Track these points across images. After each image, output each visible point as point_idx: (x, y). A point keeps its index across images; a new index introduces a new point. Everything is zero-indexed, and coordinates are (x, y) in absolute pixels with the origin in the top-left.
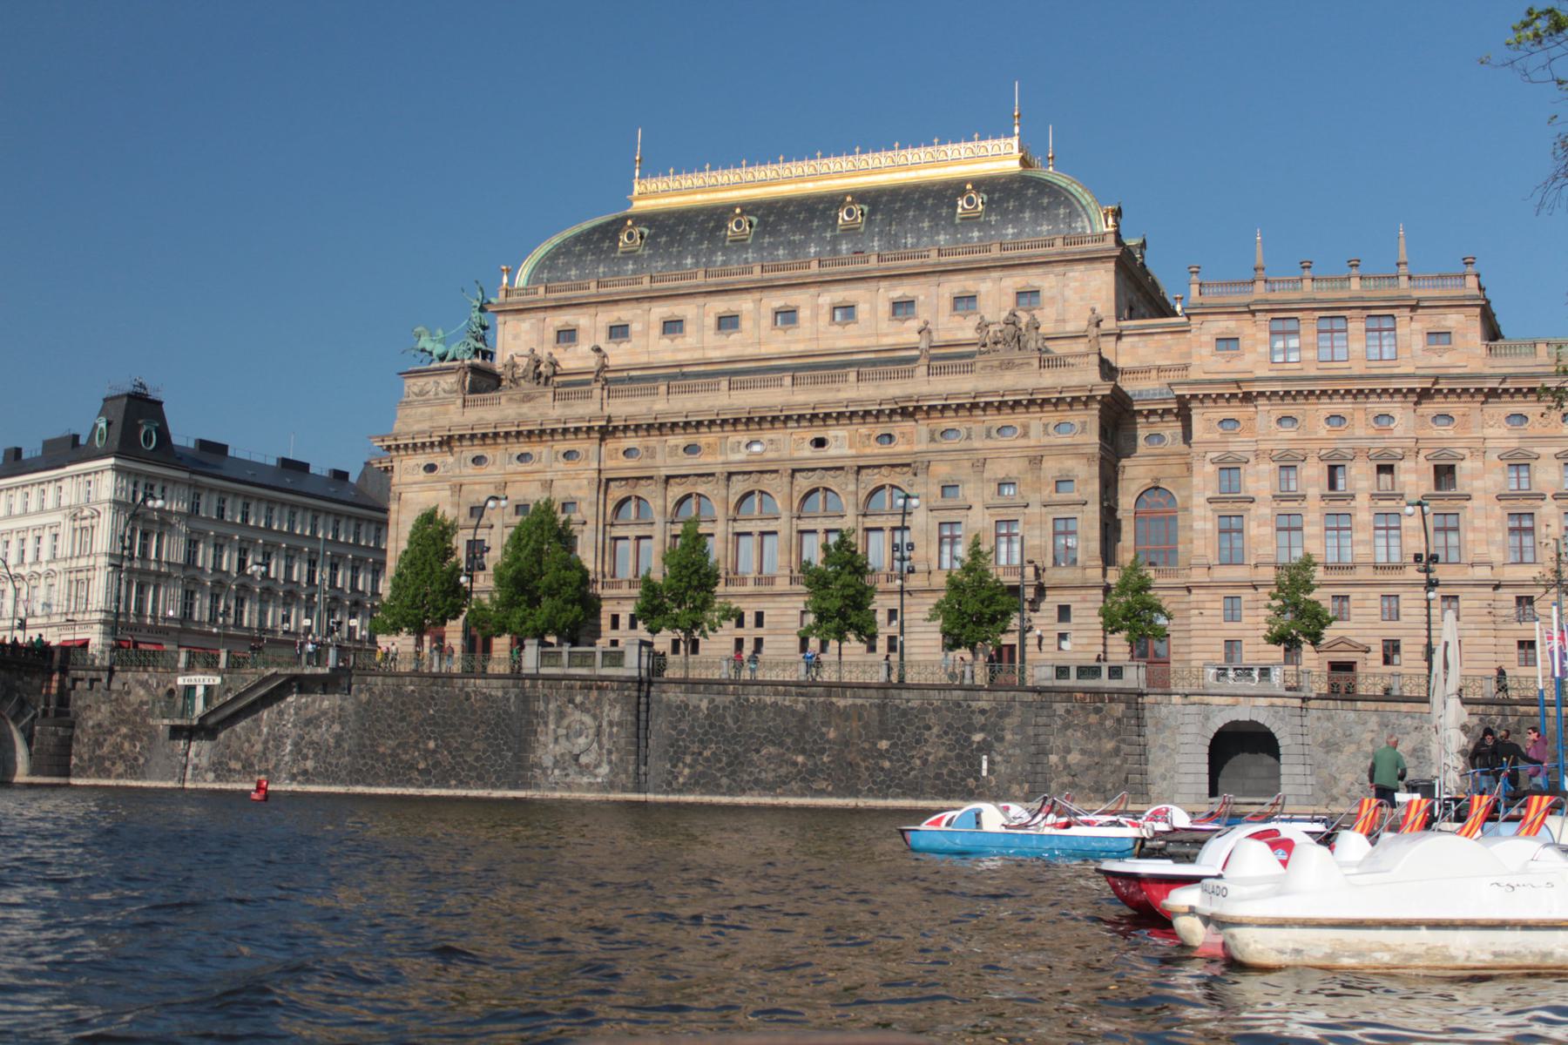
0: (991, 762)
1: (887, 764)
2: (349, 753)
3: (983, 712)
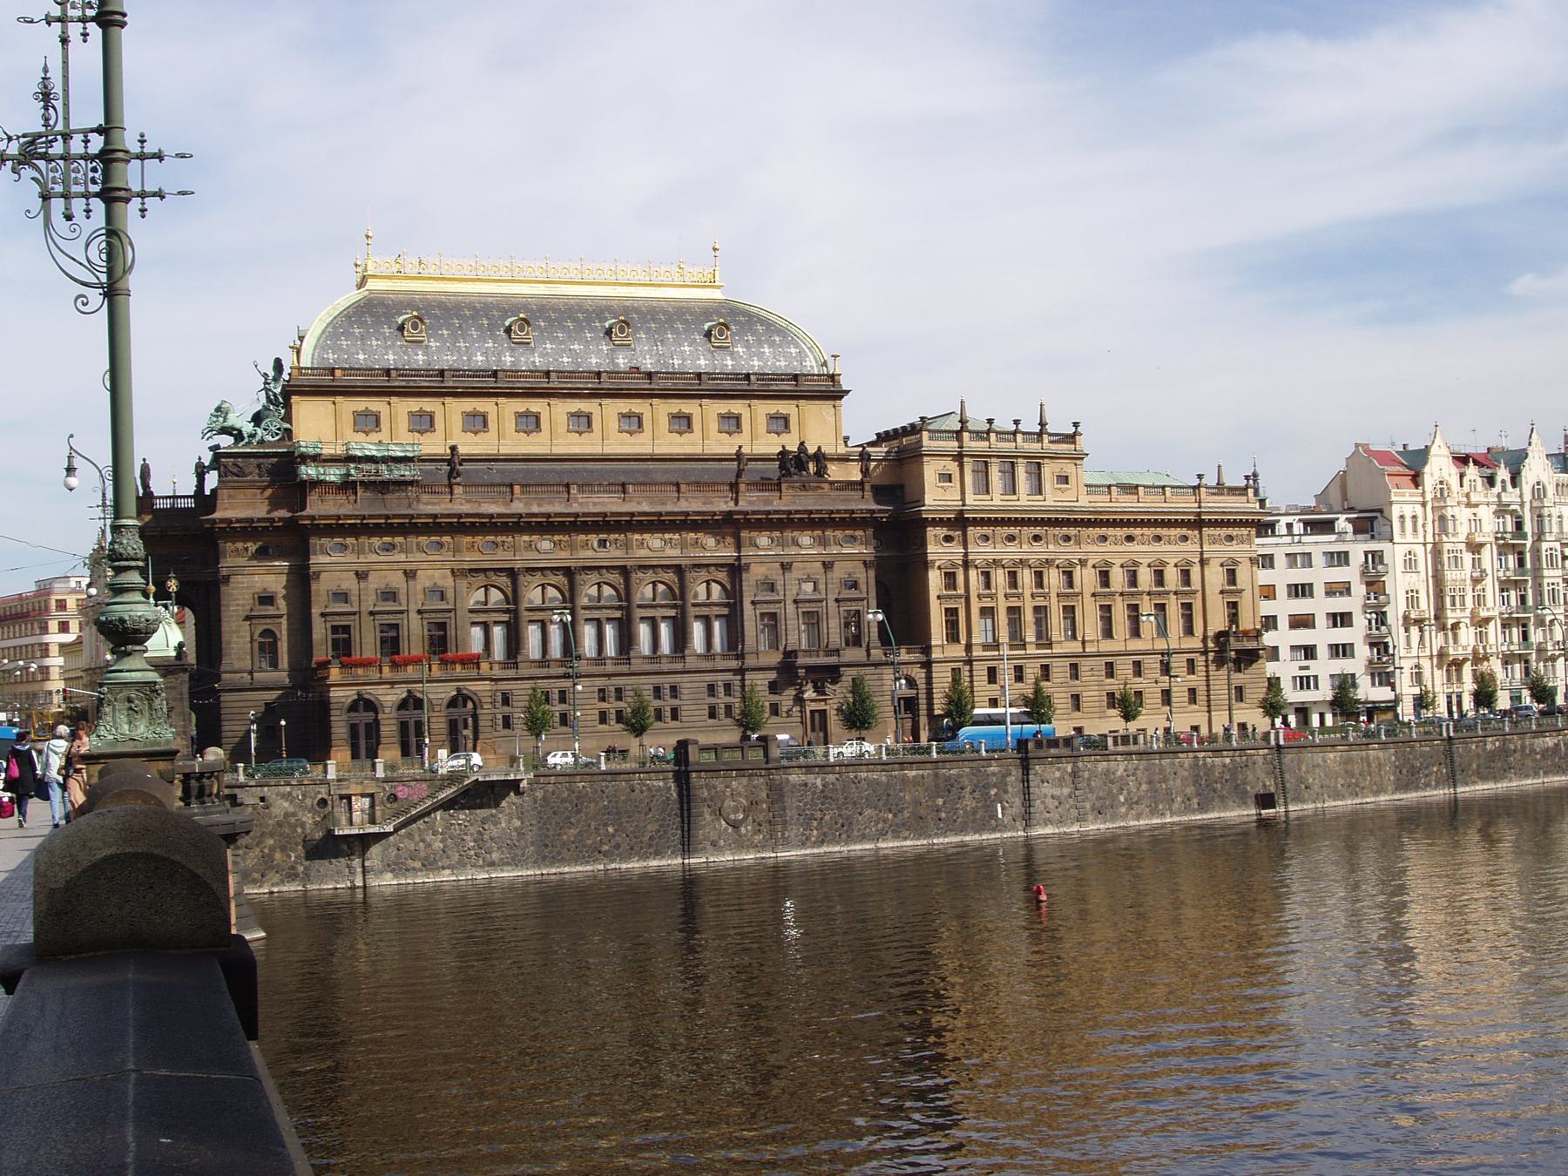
0: (1003, 809)
1: (943, 815)
2: (532, 844)
3: (994, 774)
